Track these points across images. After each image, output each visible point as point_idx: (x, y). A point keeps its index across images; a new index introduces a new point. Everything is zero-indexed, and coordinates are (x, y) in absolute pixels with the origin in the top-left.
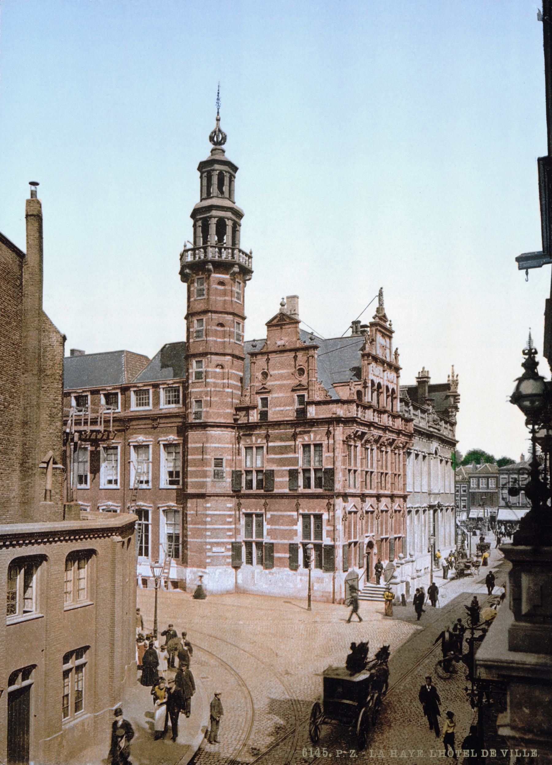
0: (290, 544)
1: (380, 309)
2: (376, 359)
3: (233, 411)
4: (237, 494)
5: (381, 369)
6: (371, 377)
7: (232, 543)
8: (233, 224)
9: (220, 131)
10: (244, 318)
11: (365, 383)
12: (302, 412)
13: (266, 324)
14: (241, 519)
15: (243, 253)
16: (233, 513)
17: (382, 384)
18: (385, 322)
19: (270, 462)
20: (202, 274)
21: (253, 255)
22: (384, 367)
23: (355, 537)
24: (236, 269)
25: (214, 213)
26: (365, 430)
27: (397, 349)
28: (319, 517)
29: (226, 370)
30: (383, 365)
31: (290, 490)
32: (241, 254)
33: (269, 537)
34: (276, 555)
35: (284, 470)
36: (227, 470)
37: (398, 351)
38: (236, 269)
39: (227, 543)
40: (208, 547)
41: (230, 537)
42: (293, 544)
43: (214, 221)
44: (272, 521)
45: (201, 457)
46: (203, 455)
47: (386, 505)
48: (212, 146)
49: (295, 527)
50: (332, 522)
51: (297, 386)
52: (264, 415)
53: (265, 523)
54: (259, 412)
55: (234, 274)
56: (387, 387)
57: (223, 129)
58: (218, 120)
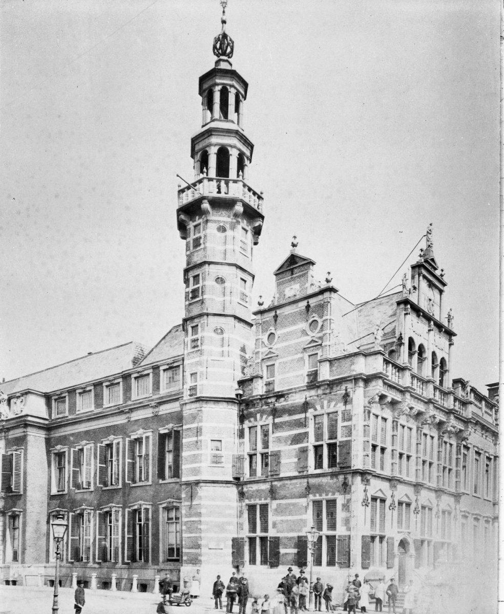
0: (299, 537)
3: (237, 386)
5: (426, 328)
8: (239, 155)
9: (225, 36)
15: (250, 189)
17: (426, 347)
18: (435, 269)
20: (199, 219)
22: (430, 326)
24: (239, 208)
25: (214, 140)
26: (398, 397)
29: (225, 335)
30: (429, 322)
31: (299, 472)
34: (282, 551)
38: (239, 208)
42: (301, 537)
44: (279, 511)
45: (195, 439)
46: (197, 436)
48: (216, 58)
51: (310, 343)
54: (265, 383)
55: (236, 215)
56: (434, 354)
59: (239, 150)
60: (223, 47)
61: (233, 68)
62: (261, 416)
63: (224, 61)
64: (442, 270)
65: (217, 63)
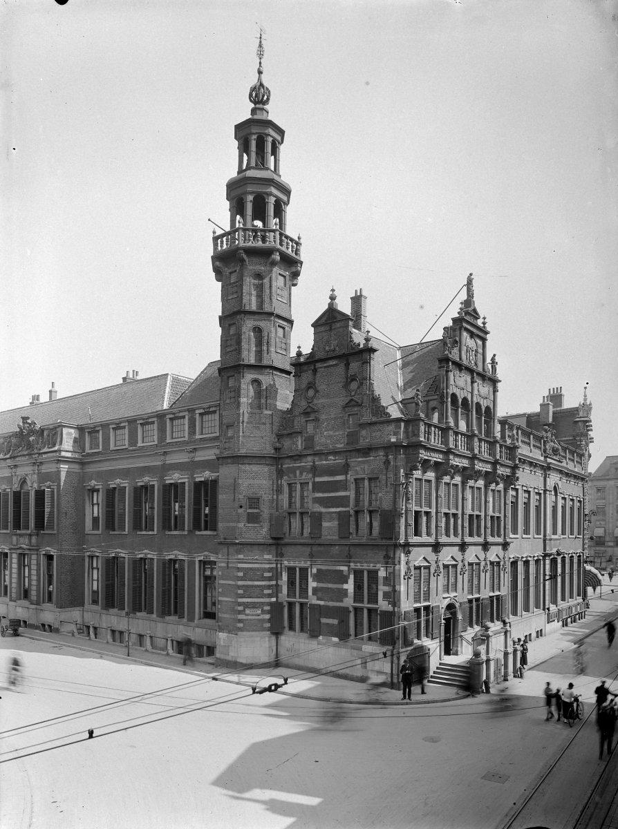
1: (468, 303)
2: (459, 366)
4: (277, 543)
6: (452, 389)
7: (271, 604)
9: (262, 85)
10: (291, 322)
11: (442, 397)
12: (353, 437)
13: (312, 325)
14: (283, 573)
16: (274, 566)
19: (317, 502)
21: (302, 241)
23: (427, 599)
27: (494, 355)
28: (373, 574)
32: (283, 238)
33: (315, 597)
35: (333, 512)
36: (266, 511)
37: (496, 357)
39: (263, 604)
40: (241, 608)
41: (270, 596)
43: (250, 198)
47: (497, 555)
48: (253, 105)
49: (345, 586)
50: (392, 580)
52: (310, 441)
53: (310, 579)
57: (265, 84)
58: (260, 72)
59: (275, 196)
60: (259, 96)
61: (270, 118)
62: (301, 474)
63: (259, 109)
64: (484, 318)
65: (254, 111)
